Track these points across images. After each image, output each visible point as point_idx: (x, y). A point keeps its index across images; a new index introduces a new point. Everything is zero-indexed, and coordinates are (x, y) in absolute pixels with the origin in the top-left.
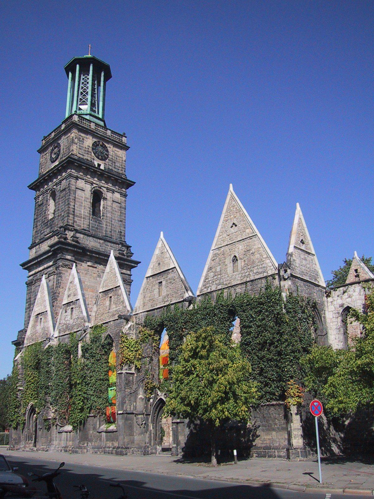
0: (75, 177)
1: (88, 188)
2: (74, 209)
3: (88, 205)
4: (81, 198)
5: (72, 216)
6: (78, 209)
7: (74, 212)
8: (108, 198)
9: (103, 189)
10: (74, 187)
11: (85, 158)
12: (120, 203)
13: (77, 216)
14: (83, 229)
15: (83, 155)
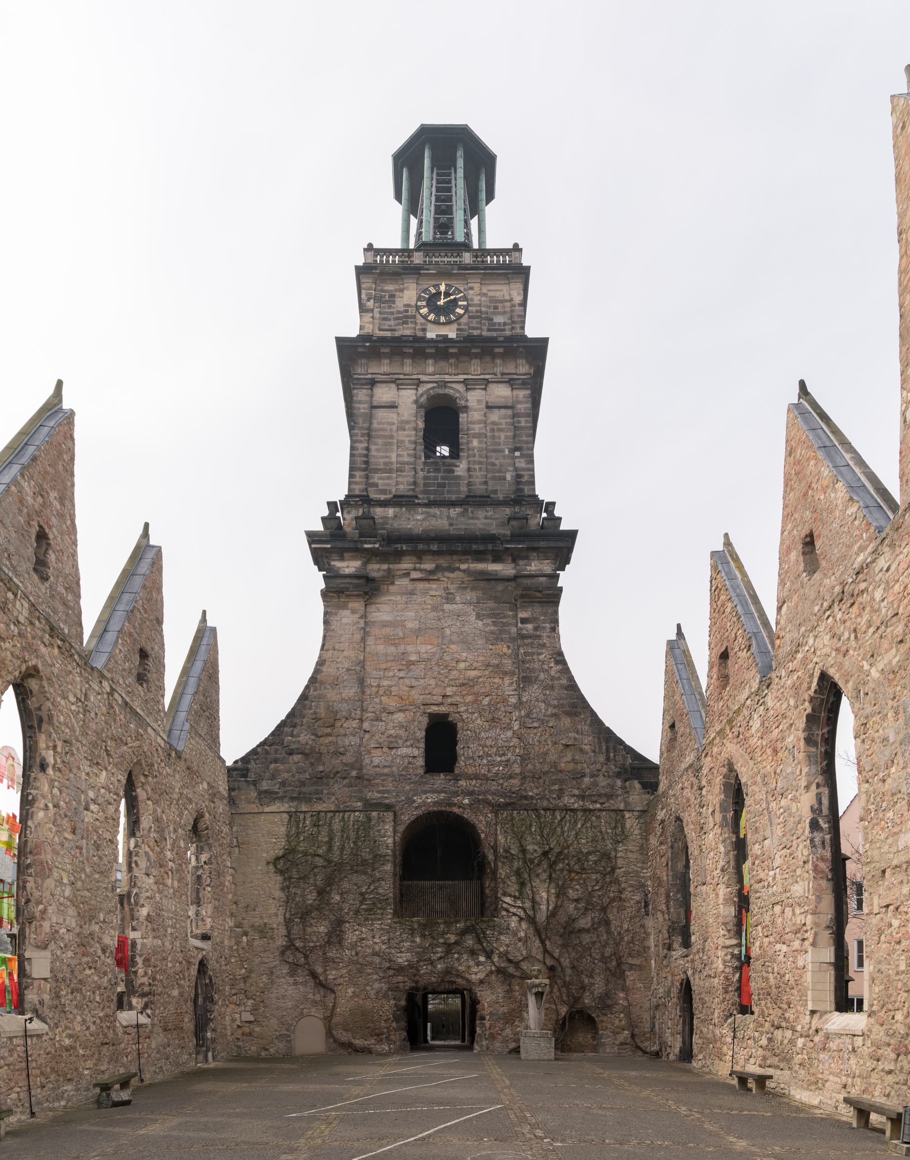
0: (366, 384)
1: (407, 398)
2: (367, 456)
3: (408, 436)
4: (389, 427)
5: (363, 473)
6: (382, 454)
7: (367, 463)
8: (469, 404)
9: (453, 389)
10: (366, 406)
11: (397, 334)
12: (511, 407)
13: (377, 471)
14: (395, 496)
15: (394, 330)
